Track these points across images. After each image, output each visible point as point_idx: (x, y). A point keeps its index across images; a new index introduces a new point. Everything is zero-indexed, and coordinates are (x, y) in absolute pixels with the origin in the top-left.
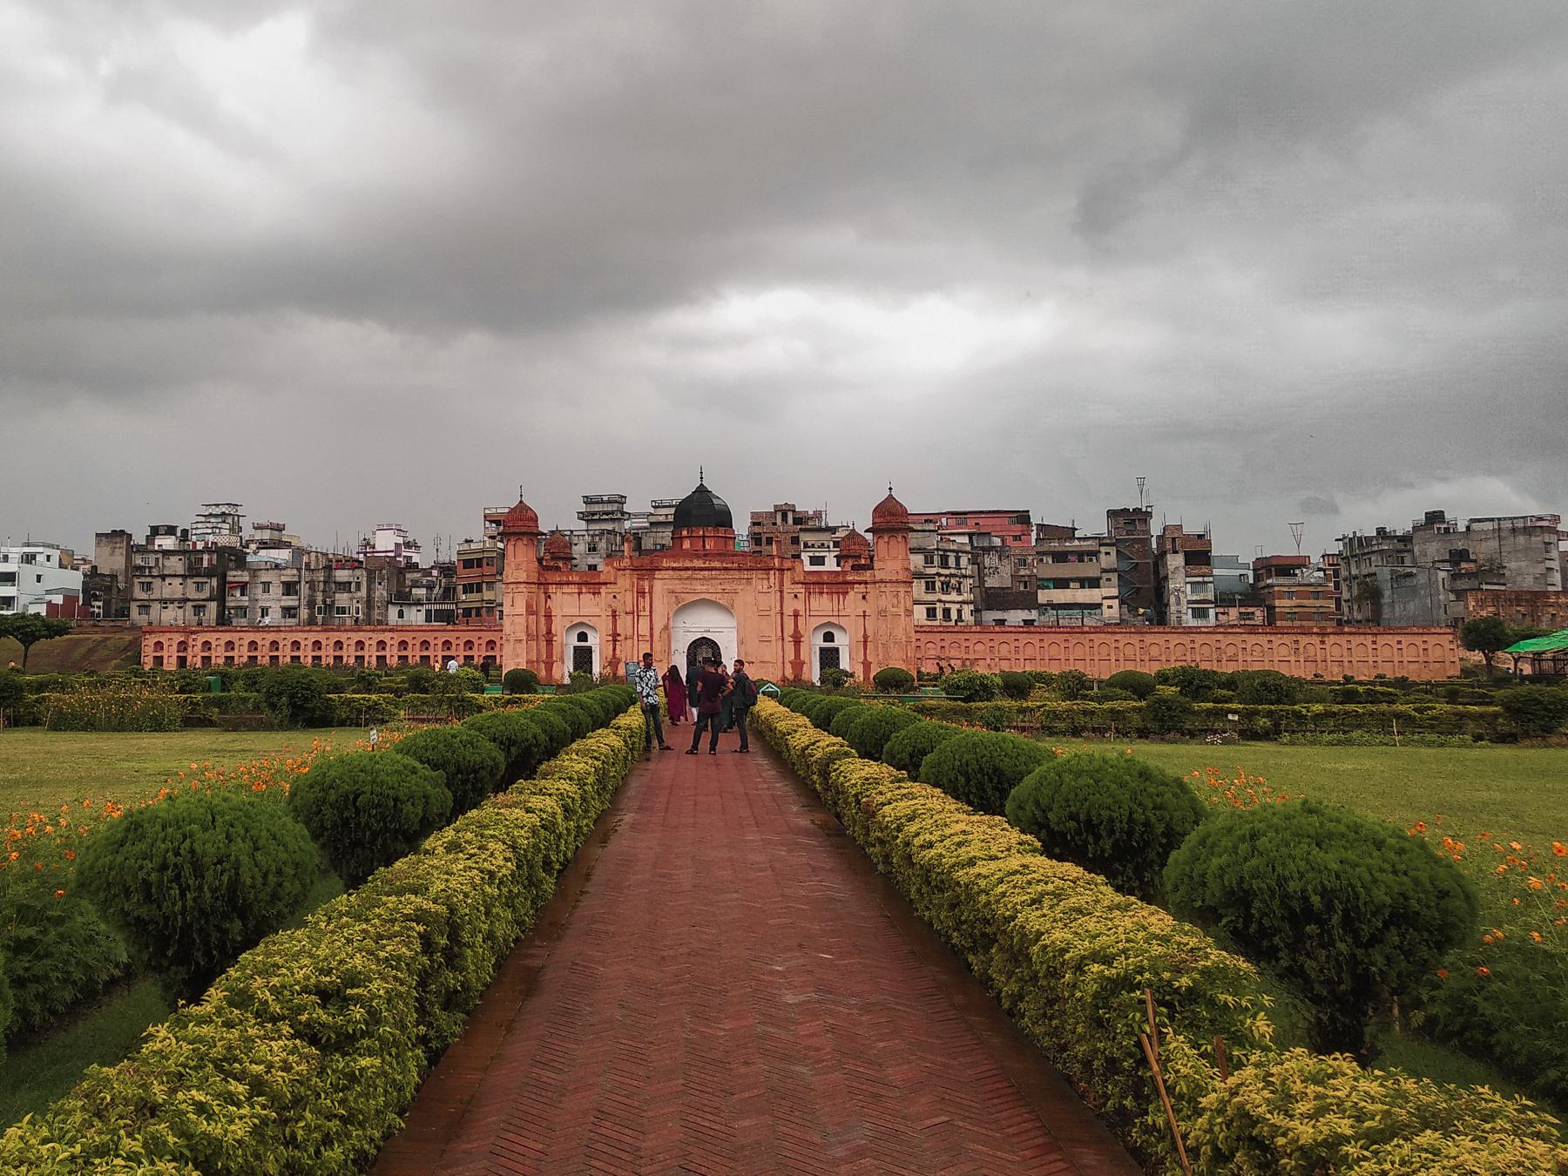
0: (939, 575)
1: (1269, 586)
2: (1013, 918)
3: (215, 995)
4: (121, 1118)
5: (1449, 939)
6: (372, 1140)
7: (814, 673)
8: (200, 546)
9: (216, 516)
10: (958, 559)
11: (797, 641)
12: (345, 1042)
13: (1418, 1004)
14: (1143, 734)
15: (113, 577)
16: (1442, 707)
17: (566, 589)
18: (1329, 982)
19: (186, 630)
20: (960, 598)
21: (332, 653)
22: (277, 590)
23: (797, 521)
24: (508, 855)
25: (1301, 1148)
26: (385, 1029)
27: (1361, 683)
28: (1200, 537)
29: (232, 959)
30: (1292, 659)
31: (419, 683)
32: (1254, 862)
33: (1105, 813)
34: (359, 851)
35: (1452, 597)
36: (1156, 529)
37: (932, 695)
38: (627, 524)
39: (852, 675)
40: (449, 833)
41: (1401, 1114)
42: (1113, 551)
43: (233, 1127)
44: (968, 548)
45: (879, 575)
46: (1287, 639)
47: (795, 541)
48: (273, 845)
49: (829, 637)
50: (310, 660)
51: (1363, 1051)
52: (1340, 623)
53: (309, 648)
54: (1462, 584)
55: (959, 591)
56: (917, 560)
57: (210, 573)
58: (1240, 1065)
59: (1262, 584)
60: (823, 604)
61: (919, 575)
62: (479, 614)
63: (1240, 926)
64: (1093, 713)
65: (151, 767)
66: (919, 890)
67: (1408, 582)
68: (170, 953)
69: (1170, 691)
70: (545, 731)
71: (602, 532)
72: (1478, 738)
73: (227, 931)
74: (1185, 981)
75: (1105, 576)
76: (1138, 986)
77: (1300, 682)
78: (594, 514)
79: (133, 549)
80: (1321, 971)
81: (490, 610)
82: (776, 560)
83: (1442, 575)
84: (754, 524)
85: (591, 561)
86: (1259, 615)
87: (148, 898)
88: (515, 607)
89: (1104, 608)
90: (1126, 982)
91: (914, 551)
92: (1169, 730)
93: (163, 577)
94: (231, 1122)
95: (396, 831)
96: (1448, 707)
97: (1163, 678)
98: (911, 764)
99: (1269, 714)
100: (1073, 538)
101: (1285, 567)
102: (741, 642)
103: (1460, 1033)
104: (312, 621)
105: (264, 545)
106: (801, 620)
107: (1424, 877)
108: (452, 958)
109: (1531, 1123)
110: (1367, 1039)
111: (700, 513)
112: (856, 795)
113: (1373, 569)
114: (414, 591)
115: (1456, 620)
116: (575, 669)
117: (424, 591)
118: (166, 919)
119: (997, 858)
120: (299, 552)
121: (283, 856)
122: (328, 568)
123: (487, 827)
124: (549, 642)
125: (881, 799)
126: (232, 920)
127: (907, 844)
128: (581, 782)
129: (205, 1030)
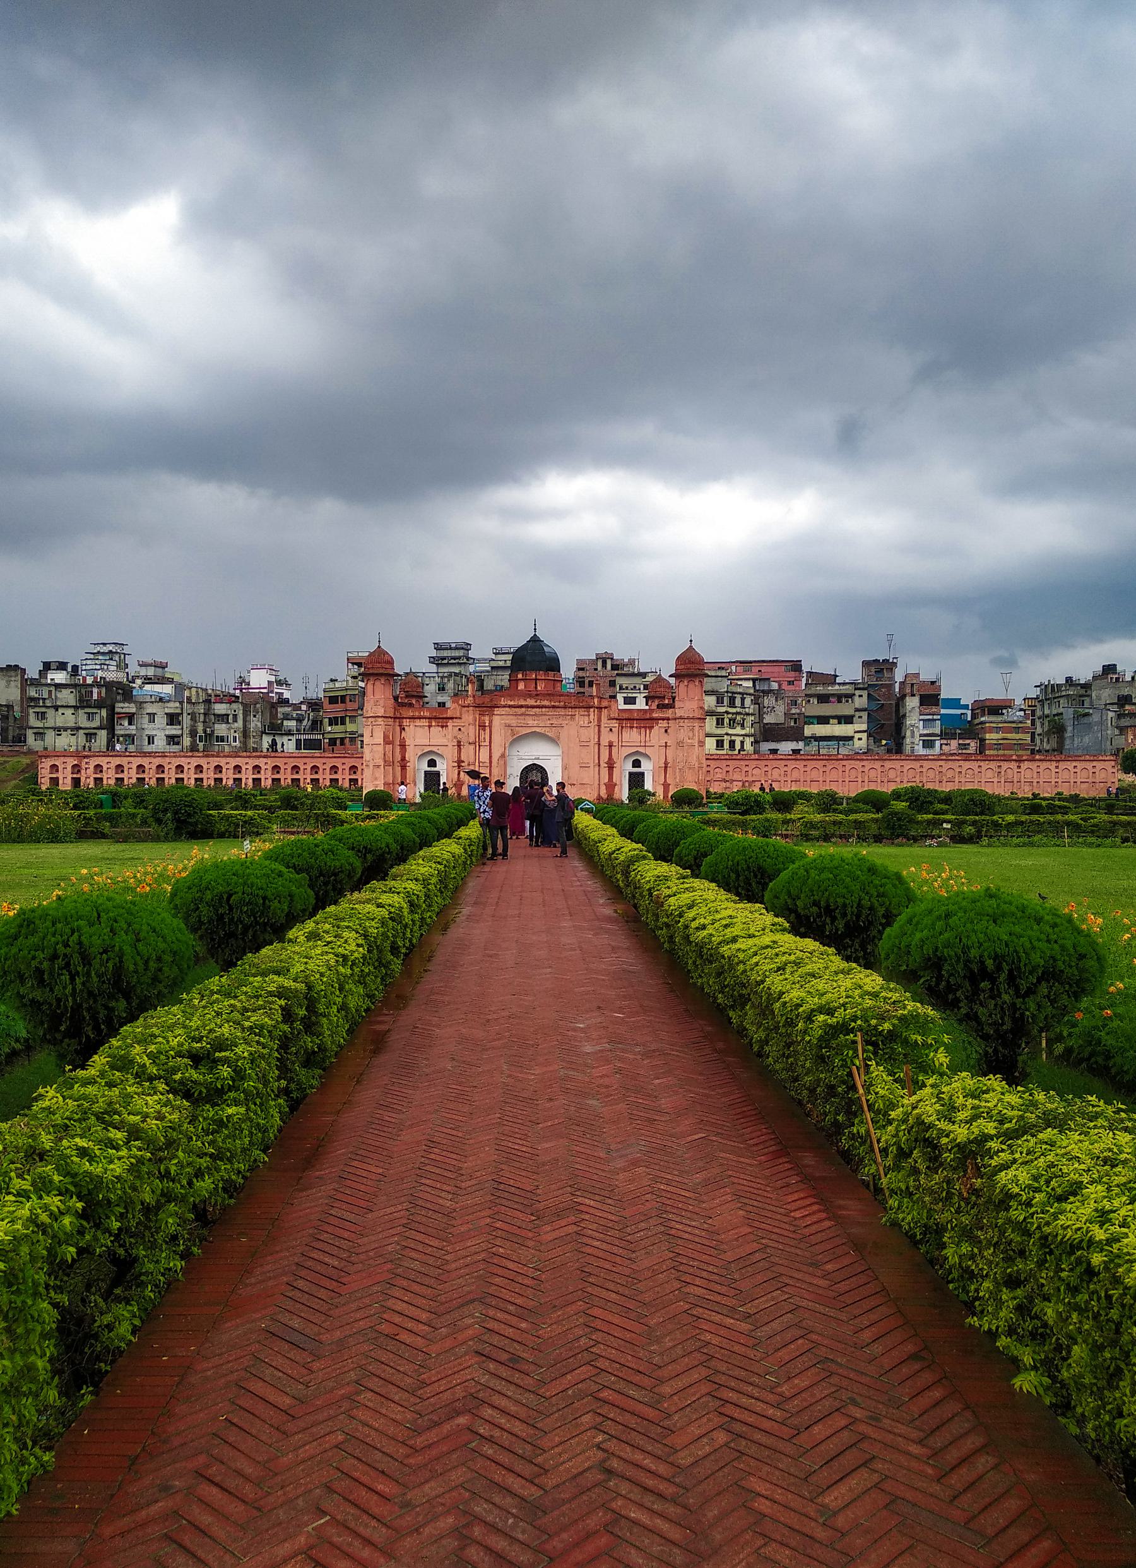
0: (727, 712)
1: (982, 723)
2: (763, 982)
3: (99, 1060)
4: (13, 1163)
5: (1083, 990)
6: (239, 1172)
7: (623, 793)
8: (89, 680)
9: (103, 654)
10: (743, 700)
11: (611, 767)
12: (215, 1095)
13: (1059, 1038)
14: (878, 839)
15: (10, 707)
16: (1103, 817)
17: (418, 723)
18: (995, 1023)
19: (77, 754)
20: (743, 732)
21: (212, 775)
22: (161, 720)
23: (615, 667)
24: (360, 942)
25: (958, 1145)
26: (249, 1084)
27: (1044, 799)
28: (933, 683)
29: (114, 1032)
30: (996, 780)
31: (289, 802)
32: (946, 935)
33: (840, 901)
34: (232, 941)
35: (1117, 732)
36: (899, 677)
37: (717, 811)
38: (472, 668)
39: (654, 795)
40: (310, 925)
41: (1031, 1117)
42: (865, 693)
43: (112, 1166)
44: (752, 691)
45: (679, 713)
46: (993, 765)
47: (612, 684)
48: (152, 937)
49: (637, 764)
50: (193, 782)
51: (1017, 1074)
52: (1033, 752)
53: (192, 771)
54: (1125, 722)
55: (743, 726)
56: (710, 701)
57: (99, 705)
58: (924, 1085)
59: (976, 721)
60: (632, 736)
61: (711, 713)
62: (342, 743)
63: (933, 984)
64: (841, 823)
65: (48, 873)
66: (694, 962)
67: (1085, 720)
68: (62, 1028)
69: (903, 805)
70: (396, 841)
71: (450, 675)
72: (1125, 840)
73: (112, 1009)
74: (887, 1026)
75: (858, 714)
76: (852, 1031)
77: (999, 798)
78: (443, 659)
79: (26, 683)
80: (990, 1016)
81: (353, 740)
82: (596, 700)
83: (1111, 714)
84: (579, 669)
85: (440, 699)
86: (973, 745)
87: (41, 982)
88: (373, 738)
89: (856, 740)
90: (844, 1028)
91: (707, 693)
92: (898, 837)
93: (56, 708)
94: (111, 1162)
95: (265, 924)
96: (1106, 817)
97: (897, 796)
98: (694, 866)
99: (974, 823)
100: (834, 683)
101: (995, 708)
102: (565, 768)
103: (1088, 1059)
104: (193, 748)
105: (148, 680)
106: (614, 750)
107: (1069, 944)
108: (310, 1026)
109: (1122, 1121)
110: (1020, 1065)
111: (533, 659)
112: (649, 890)
113: (1061, 710)
114: (286, 723)
115: (1118, 750)
116: (426, 789)
117: (293, 723)
118: (59, 1000)
119: (754, 936)
120: (180, 687)
121: (162, 946)
122: (208, 702)
123: (343, 920)
124: (404, 768)
125: (668, 892)
126: (117, 1001)
127: (687, 927)
128: (425, 882)
129: (90, 1090)
